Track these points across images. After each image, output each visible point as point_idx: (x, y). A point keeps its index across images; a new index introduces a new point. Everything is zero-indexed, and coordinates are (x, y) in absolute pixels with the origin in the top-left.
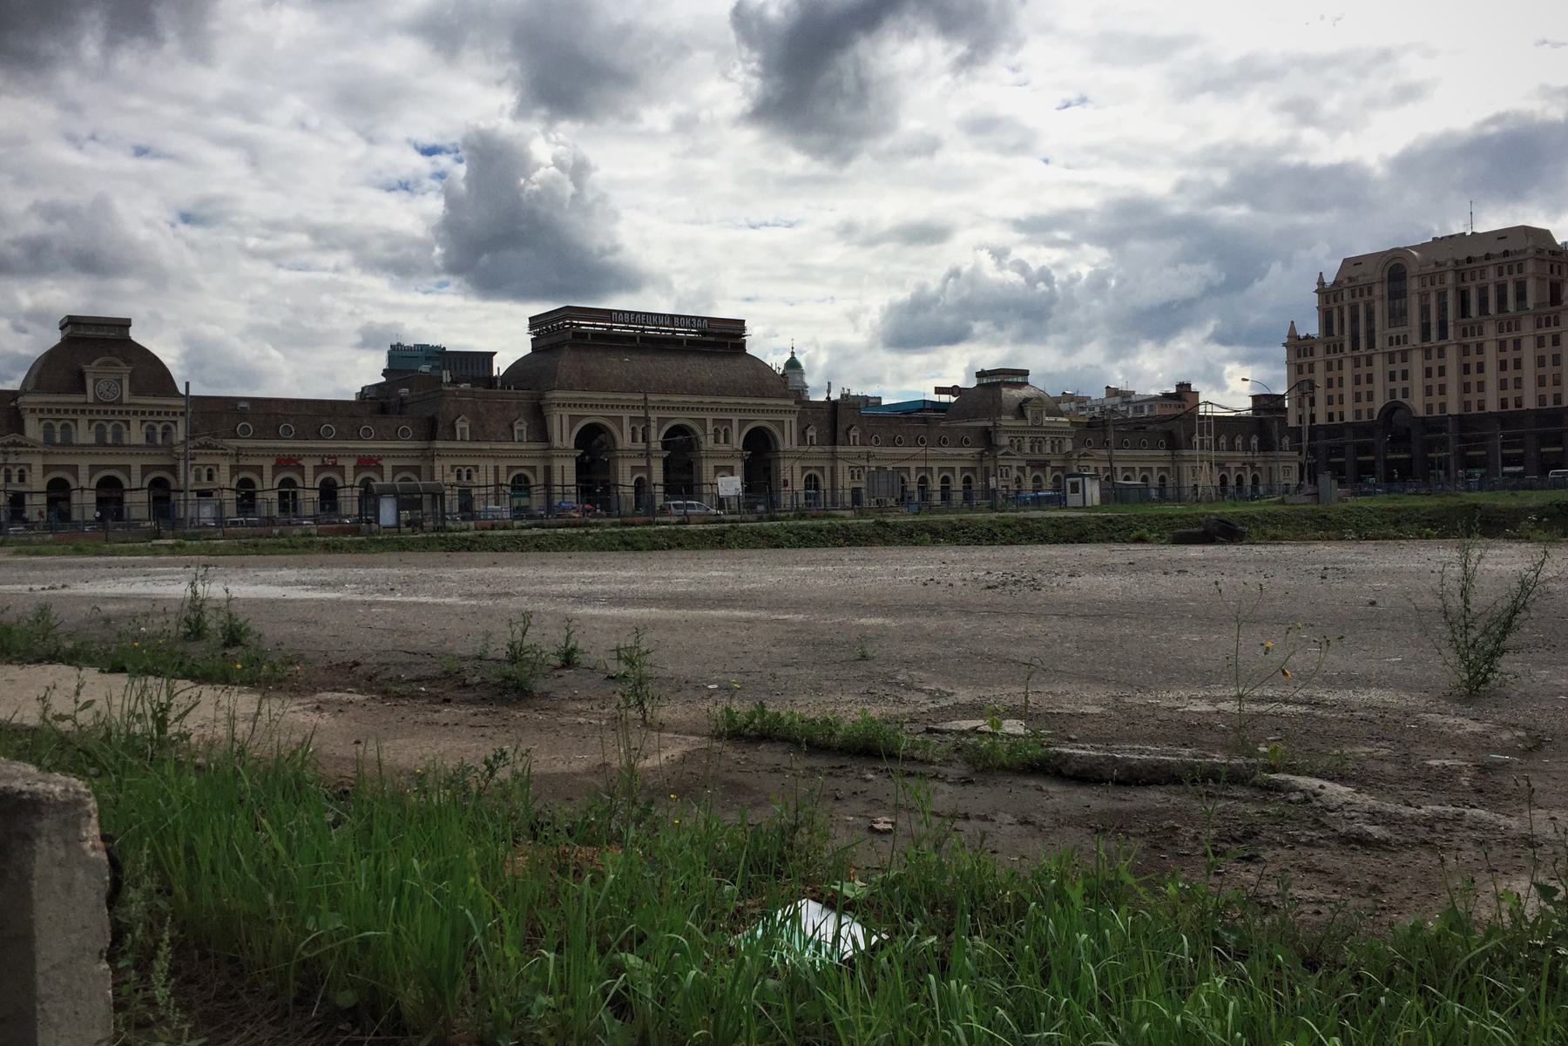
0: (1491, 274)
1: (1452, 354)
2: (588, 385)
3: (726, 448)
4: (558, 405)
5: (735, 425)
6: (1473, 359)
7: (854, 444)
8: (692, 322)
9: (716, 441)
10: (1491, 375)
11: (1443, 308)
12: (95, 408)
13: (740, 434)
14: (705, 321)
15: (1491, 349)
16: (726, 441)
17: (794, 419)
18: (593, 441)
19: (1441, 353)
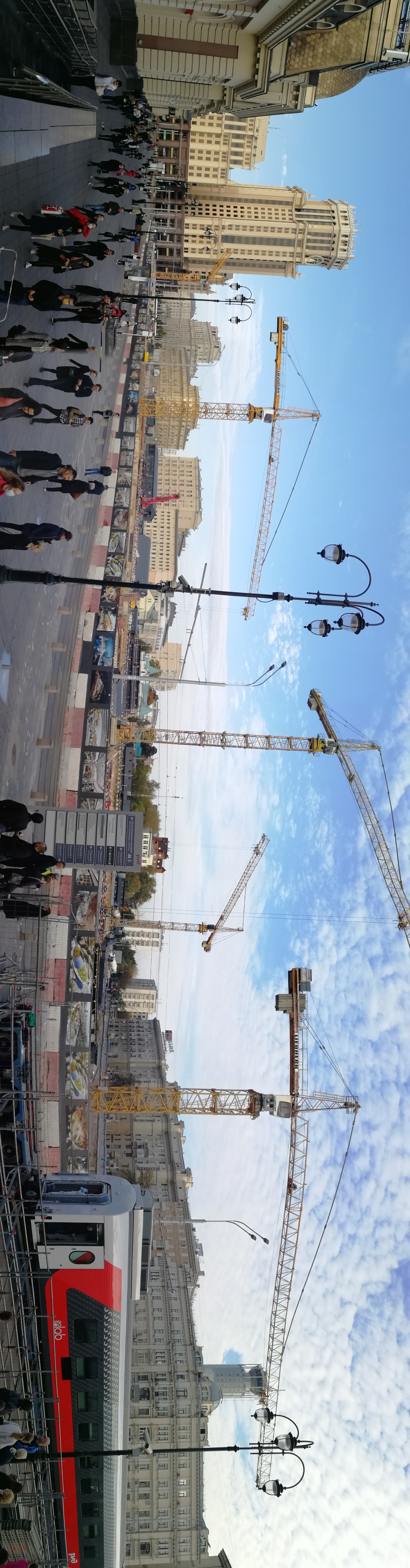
0: (248, 150)
1: (218, 130)
6: (214, 139)
10: (205, 147)
11: (239, 128)
15: (216, 148)
19: (219, 125)
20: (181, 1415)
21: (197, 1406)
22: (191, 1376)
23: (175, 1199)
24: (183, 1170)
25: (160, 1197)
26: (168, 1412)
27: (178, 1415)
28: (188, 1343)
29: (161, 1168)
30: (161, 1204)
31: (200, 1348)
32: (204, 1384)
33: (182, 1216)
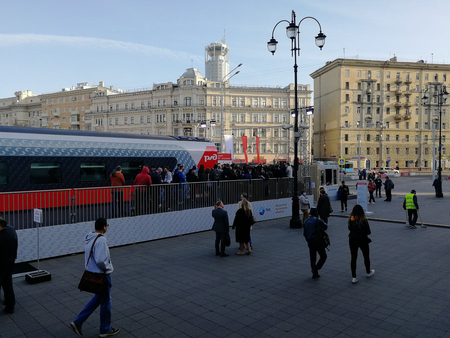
20: (204, 103)
21: (197, 89)
22: (175, 93)
23: (39, 105)
24: (17, 98)
25: (39, 118)
26: (202, 112)
27: (205, 105)
28: (150, 96)
29: (15, 117)
30: (43, 117)
31: (155, 85)
32: (182, 83)
33: (52, 100)
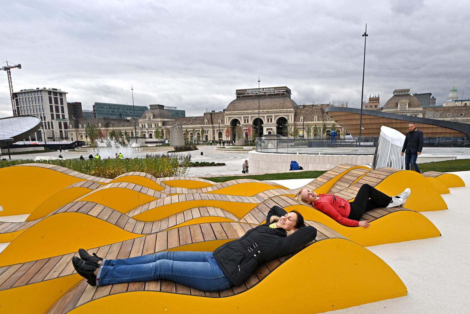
2: (234, 109)
3: (271, 123)
4: (225, 115)
5: (273, 117)
7: (316, 121)
8: (269, 89)
9: (268, 121)
12: (148, 121)
13: (275, 119)
14: (273, 88)
16: (271, 121)
17: (293, 114)
18: (235, 122)
